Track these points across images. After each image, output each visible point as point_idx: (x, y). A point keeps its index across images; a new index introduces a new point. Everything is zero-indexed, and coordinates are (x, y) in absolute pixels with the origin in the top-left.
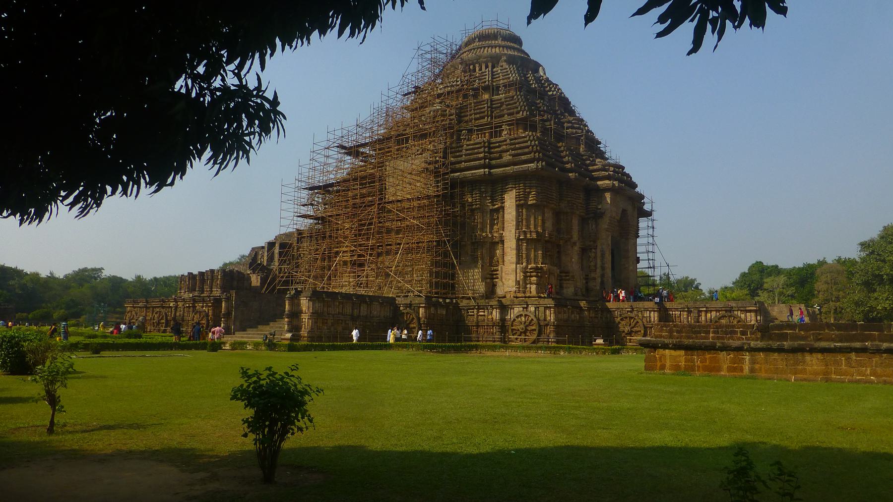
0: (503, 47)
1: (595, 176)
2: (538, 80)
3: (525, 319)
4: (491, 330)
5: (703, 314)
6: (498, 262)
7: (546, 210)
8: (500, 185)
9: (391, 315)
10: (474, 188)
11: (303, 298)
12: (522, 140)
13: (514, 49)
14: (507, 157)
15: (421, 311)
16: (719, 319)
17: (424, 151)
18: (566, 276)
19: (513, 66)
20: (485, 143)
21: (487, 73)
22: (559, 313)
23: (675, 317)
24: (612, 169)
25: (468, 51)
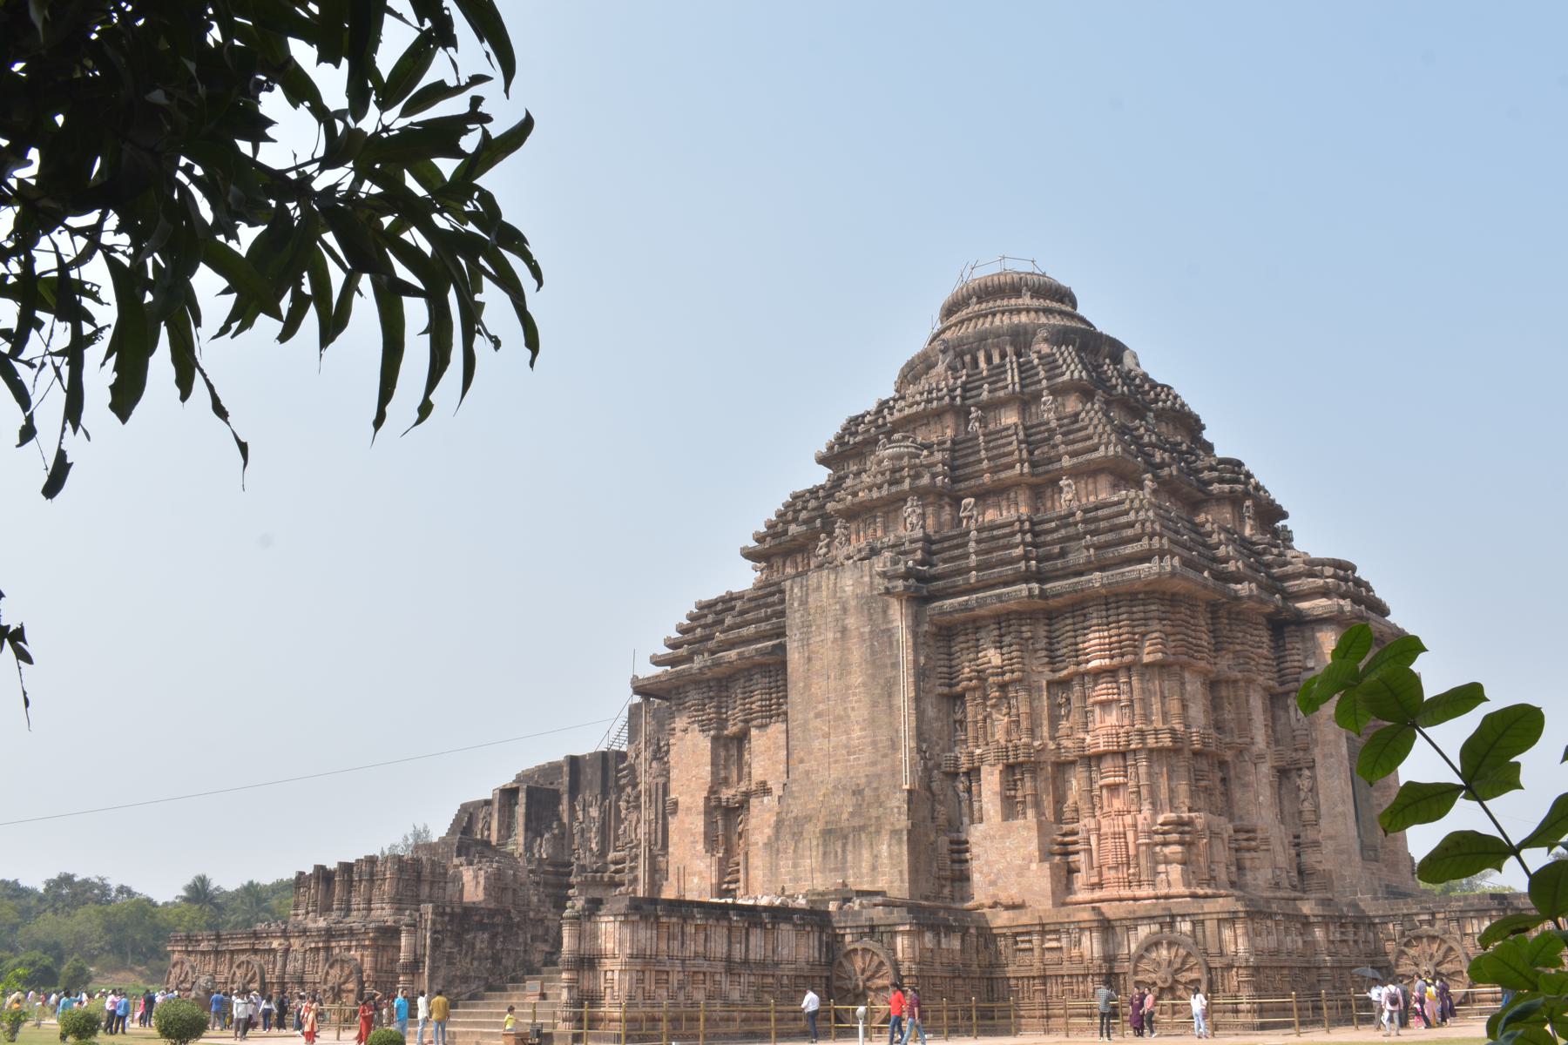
0: (1037, 311)
1: (1291, 590)
2: (1128, 377)
3: (1169, 953)
4: (1081, 988)
6: (1077, 810)
7: (1187, 675)
8: (1070, 621)
9: (823, 956)
10: (1003, 631)
11: (606, 919)
12: (1115, 509)
13: (1061, 313)
14: (1078, 557)
15: (901, 943)
17: (874, 552)
18: (1247, 840)
20: (1022, 522)
21: (1008, 366)
22: (1258, 934)
24: (1329, 571)
25: (955, 325)
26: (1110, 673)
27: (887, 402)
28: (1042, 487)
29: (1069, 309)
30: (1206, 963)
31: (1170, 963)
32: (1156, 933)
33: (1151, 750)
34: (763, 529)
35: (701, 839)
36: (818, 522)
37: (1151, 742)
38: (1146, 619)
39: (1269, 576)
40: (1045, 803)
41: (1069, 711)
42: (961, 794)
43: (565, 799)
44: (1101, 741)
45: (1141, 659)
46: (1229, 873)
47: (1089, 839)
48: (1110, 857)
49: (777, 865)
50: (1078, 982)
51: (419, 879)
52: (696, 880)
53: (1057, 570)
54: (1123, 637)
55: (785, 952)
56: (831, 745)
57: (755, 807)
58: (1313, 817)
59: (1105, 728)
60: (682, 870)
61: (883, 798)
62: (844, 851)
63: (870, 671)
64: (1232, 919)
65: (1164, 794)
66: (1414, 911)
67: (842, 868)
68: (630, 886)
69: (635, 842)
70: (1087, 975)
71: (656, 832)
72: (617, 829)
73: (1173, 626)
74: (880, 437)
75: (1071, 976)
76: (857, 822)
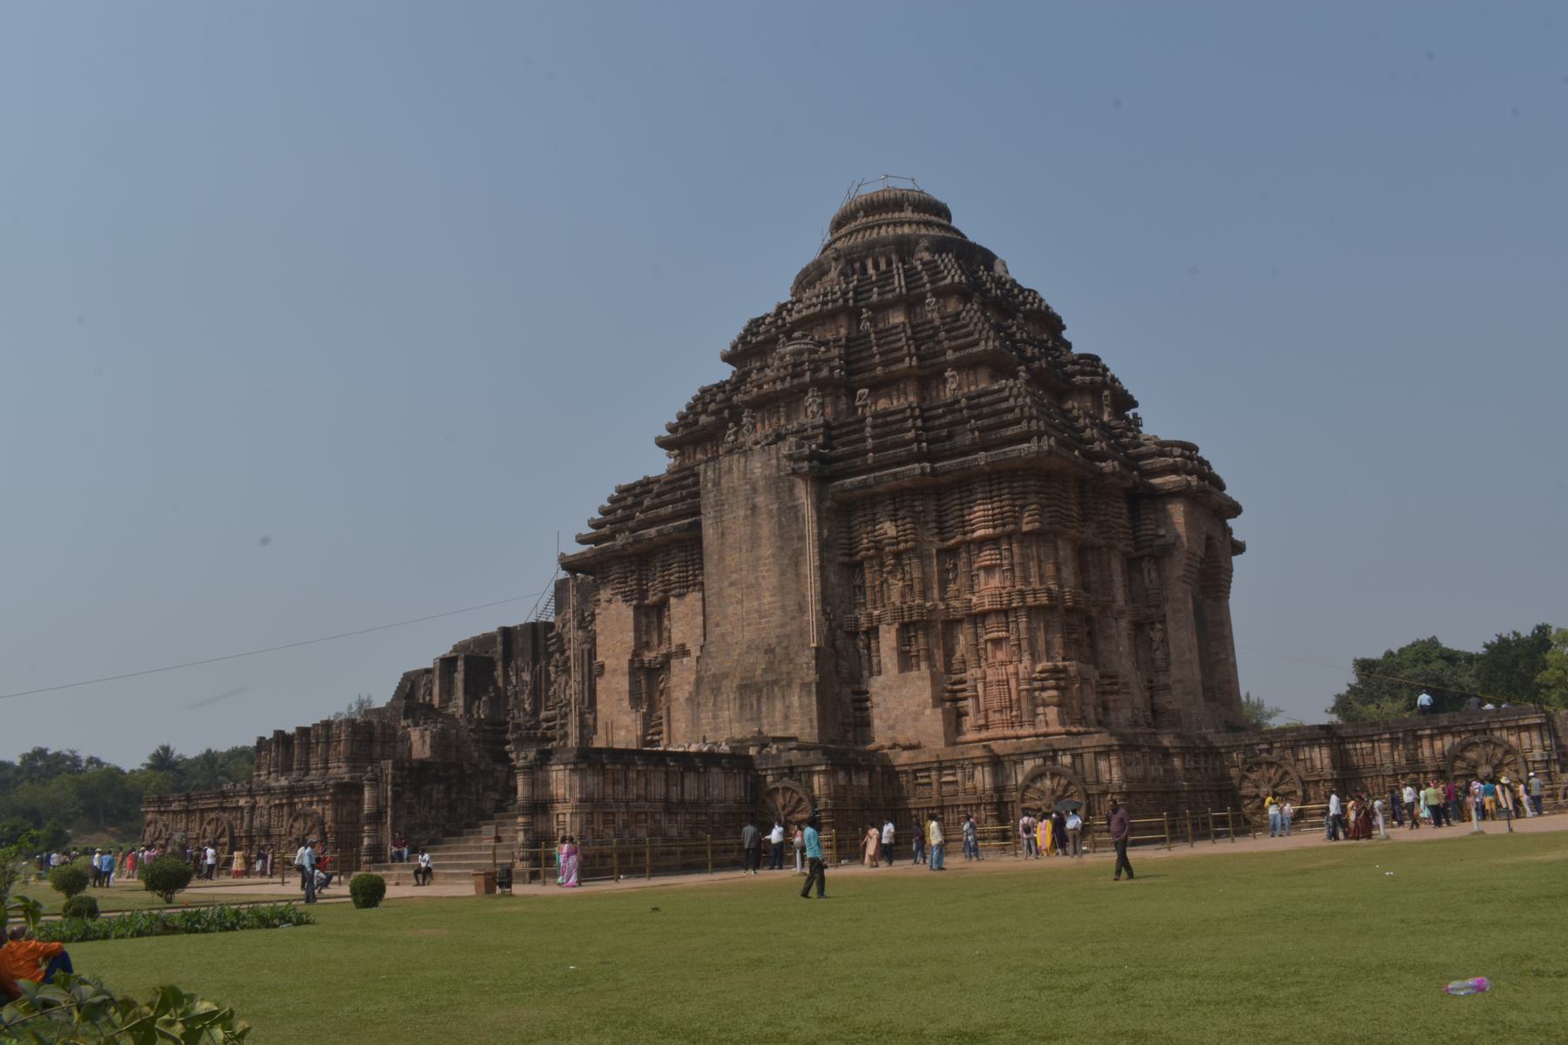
0: (918, 223)
2: (1000, 282)
5: (1426, 743)
6: (964, 662)
7: (1060, 542)
8: (957, 496)
10: (897, 505)
11: (556, 768)
13: (940, 226)
14: (965, 439)
15: (818, 781)
16: (1462, 751)
17: (779, 438)
18: (1110, 684)
19: (947, 255)
20: (913, 409)
21: (895, 271)
22: (1128, 764)
23: (1362, 755)
24: (1177, 451)
25: (845, 236)
26: (993, 541)
27: (785, 305)
28: (928, 378)
29: (945, 222)
30: (1085, 790)
31: (1053, 791)
32: (1039, 766)
33: (1030, 608)
34: (675, 421)
35: (626, 697)
36: (726, 413)
37: (1030, 600)
38: (1024, 493)
39: (1127, 456)
40: (937, 656)
41: (957, 576)
44: (986, 600)
45: (1021, 528)
46: (1096, 714)
47: (976, 686)
49: (698, 717)
52: (623, 733)
53: (946, 450)
54: (1005, 509)
55: (716, 792)
56: (745, 610)
58: (1164, 664)
59: (989, 589)
61: (792, 655)
62: (759, 702)
64: (1106, 752)
65: (1041, 646)
66: (1255, 741)
69: (565, 702)
72: (547, 690)
73: (1047, 499)
74: (781, 336)
75: (964, 805)
76: (770, 677)
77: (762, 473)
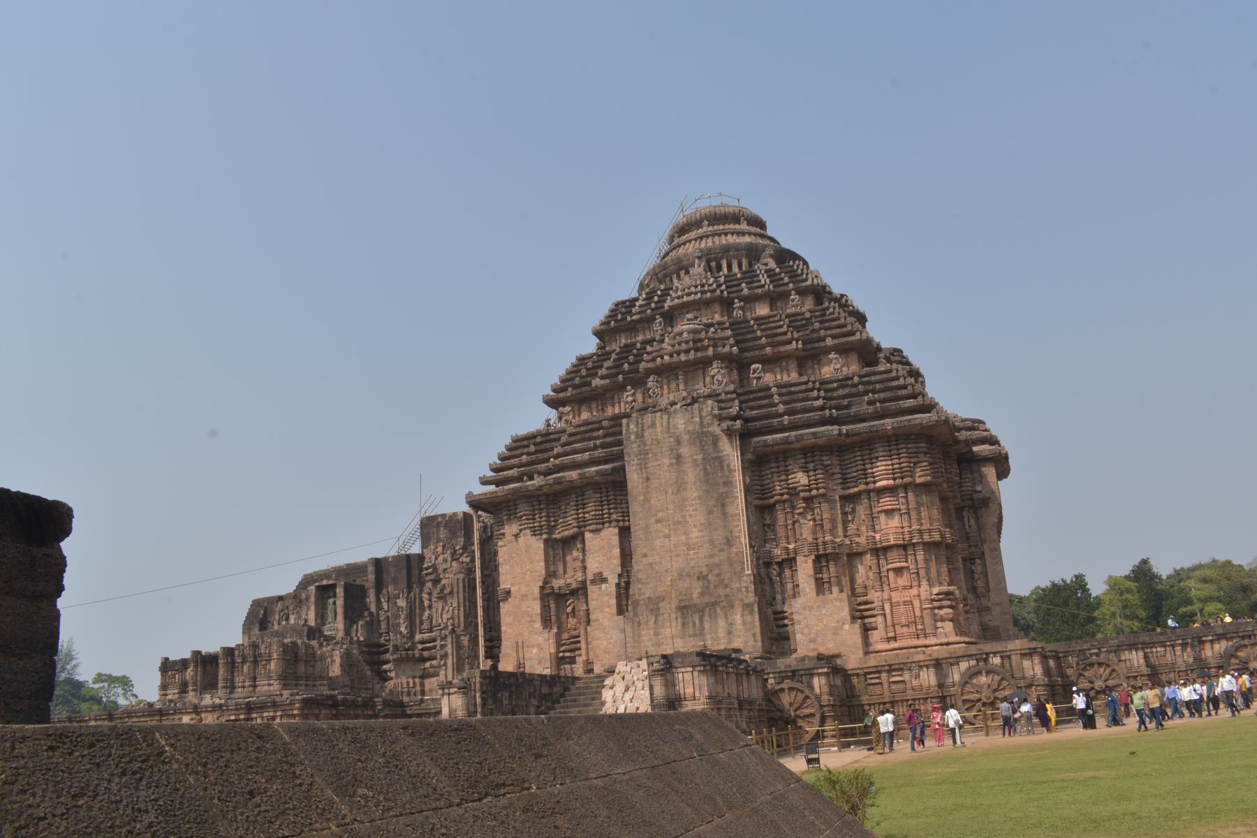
5: (1208, 646)
12: (885, 376)
16: (1236, 651)
26: (891, 490)
32: (974, 666)
33: (925, 544)
35: (539, 619)
37: (926, 538)
38: (916, 453)
41: (854, 518)
42: (774, 578)
43: (372, 594)
44: (891, 537)
45: (914, 480)
47: (883, 606)
48: (903, 618)
49: (639, 635)
50: (919, 704)
51: (296, 659)
52: (535, 651)
53: (851, 416)
56: (672, 543)
57: (594, 592)
59: (890, 528)
60: (520, 644)
61: (726, 581)
63: (704, 488)
64: (1029, 654)
65: (933, 574)
66: (1085, 648)
67: (701, 634)
68: (441, 660)
69: (442, 626)
70: (927, 698)
71: (459, 618)
72: (421, 615)
74: (657, 317)
75: (914, 700)
76: (707, 599)
77: (685, 428)
